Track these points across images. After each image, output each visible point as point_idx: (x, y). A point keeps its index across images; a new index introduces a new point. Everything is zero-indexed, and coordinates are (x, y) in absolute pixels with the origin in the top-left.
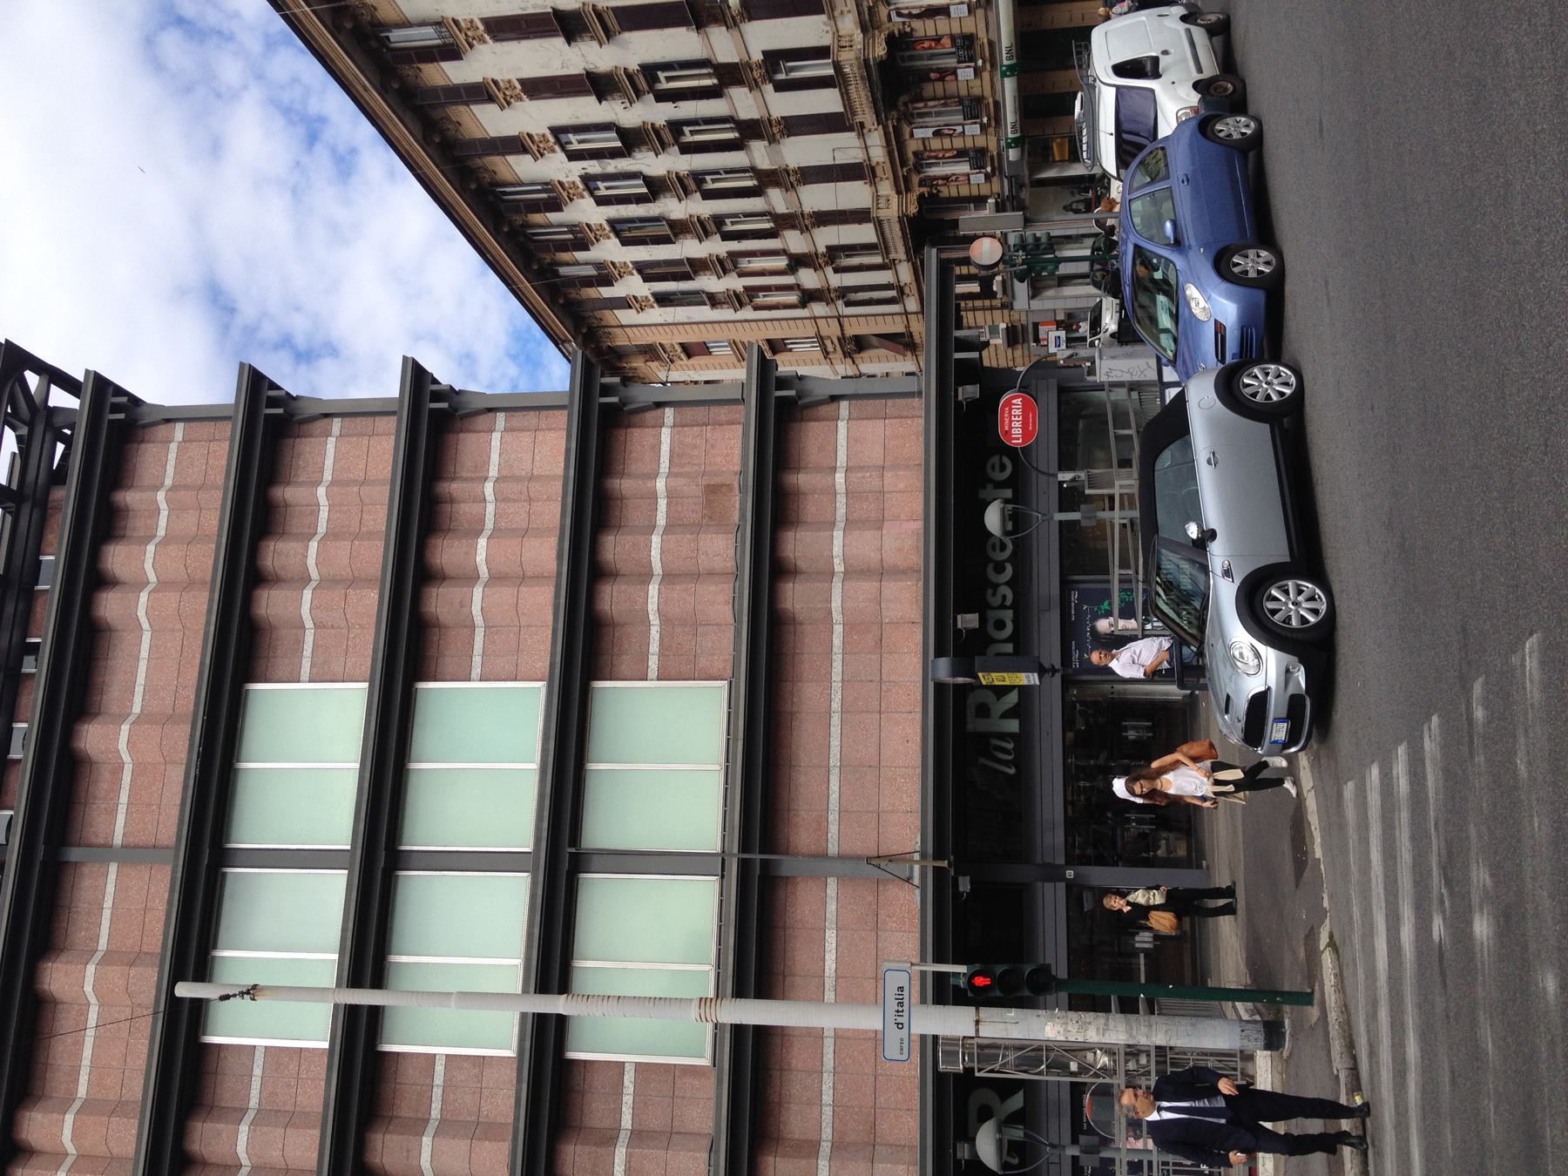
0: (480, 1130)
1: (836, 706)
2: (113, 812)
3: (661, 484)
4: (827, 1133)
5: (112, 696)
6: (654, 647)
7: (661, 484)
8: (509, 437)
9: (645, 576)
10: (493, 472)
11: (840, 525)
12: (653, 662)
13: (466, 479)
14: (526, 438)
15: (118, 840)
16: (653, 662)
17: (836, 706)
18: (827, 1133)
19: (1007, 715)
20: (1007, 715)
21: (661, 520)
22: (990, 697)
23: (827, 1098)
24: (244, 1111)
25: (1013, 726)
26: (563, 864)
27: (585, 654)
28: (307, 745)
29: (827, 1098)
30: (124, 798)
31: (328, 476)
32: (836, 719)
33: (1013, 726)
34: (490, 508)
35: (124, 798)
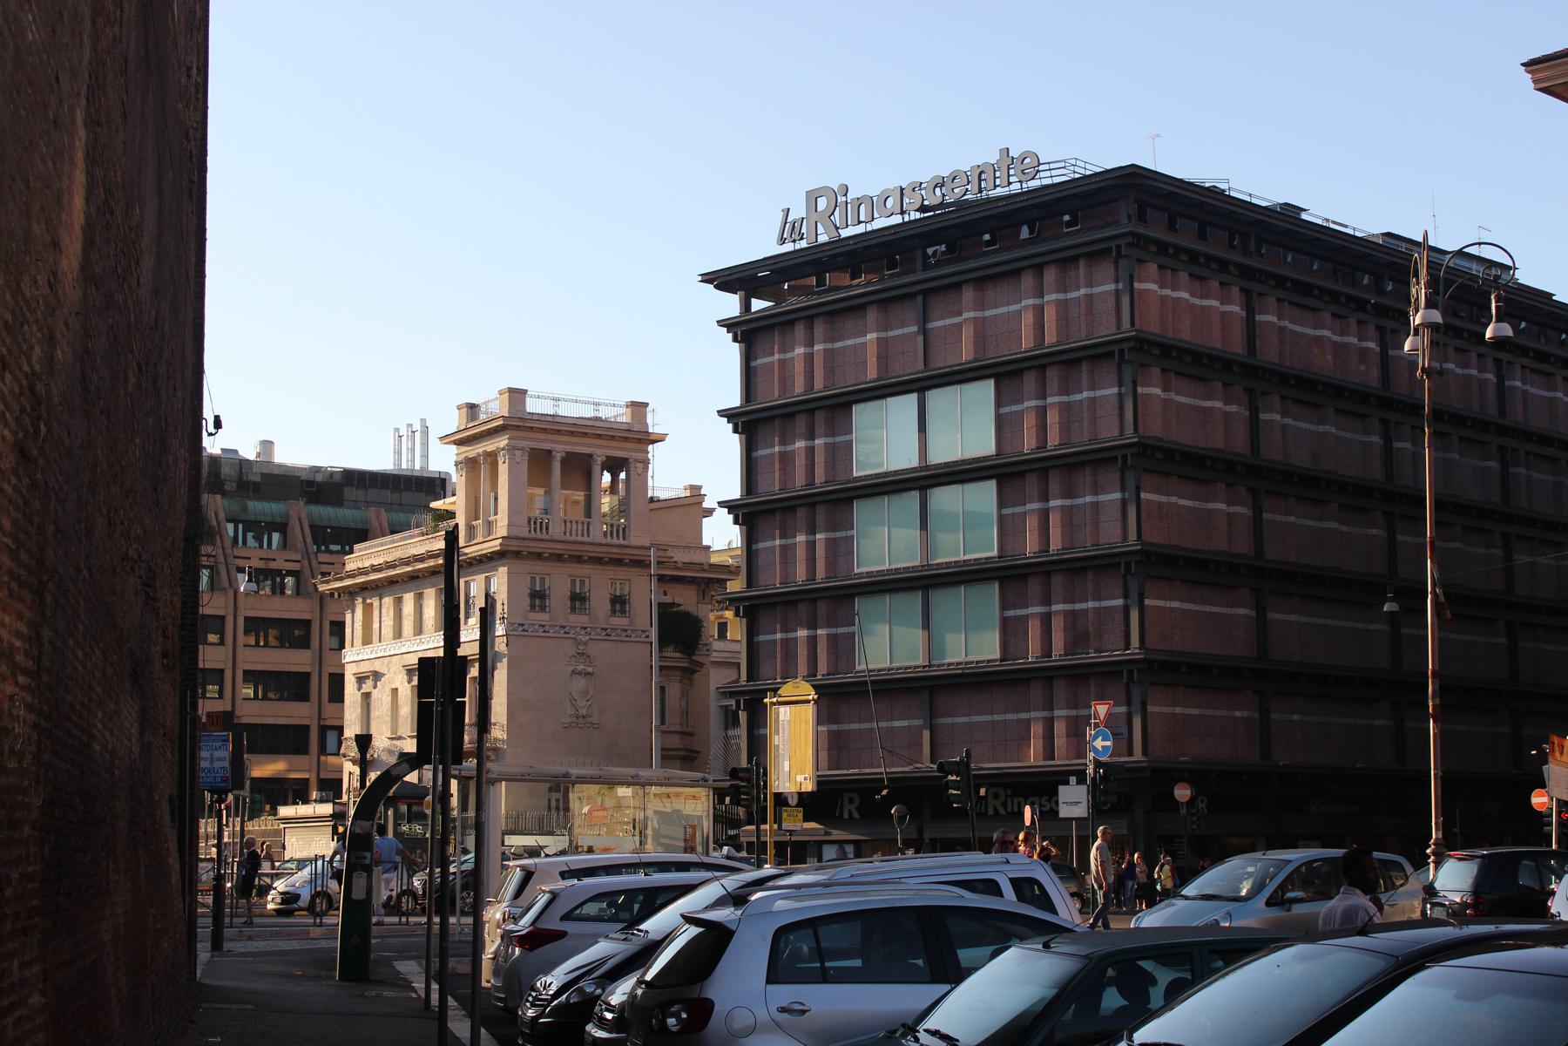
0: (831, 563)
1: (996, 717)
2: (942, 318)
3: (1091, 604)
4: (845, 727)
5: (991, 294)
6: (1019, 612)
7: (1091, 604)
8: (1118, 506)
9: (1047, 601)
10: (1102, 498)
11: (1073, 713)
12: (1011, 613)
13: (1095, 483)
14: (1118, 515)
15: (931, 325)
16: (1011, 613)
17: (996, 717)
18: (845, 727)
19: (995, 809)
20: (995, 809)
21: (1079, 606)
22: (1002, 799)
23: (853, 726)
24: (833, 435)
25: (991, 812)
26: (925, 582)
27: (1008, 576)
28: (966, 424)
29: (853, 726)
30: (948, 322)
31: (1099, 393)
32: (988, 718)
33: (991, 812)
34: (1080, 501)
35: (948, 322)
